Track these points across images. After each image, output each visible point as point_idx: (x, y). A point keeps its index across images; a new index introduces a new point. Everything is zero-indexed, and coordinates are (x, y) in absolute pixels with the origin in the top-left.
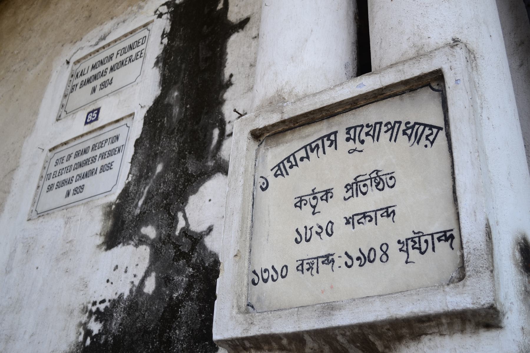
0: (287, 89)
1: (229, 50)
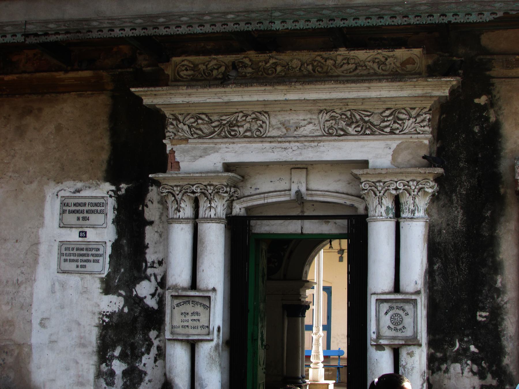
0: (178, 284)
1: (146, 232)
